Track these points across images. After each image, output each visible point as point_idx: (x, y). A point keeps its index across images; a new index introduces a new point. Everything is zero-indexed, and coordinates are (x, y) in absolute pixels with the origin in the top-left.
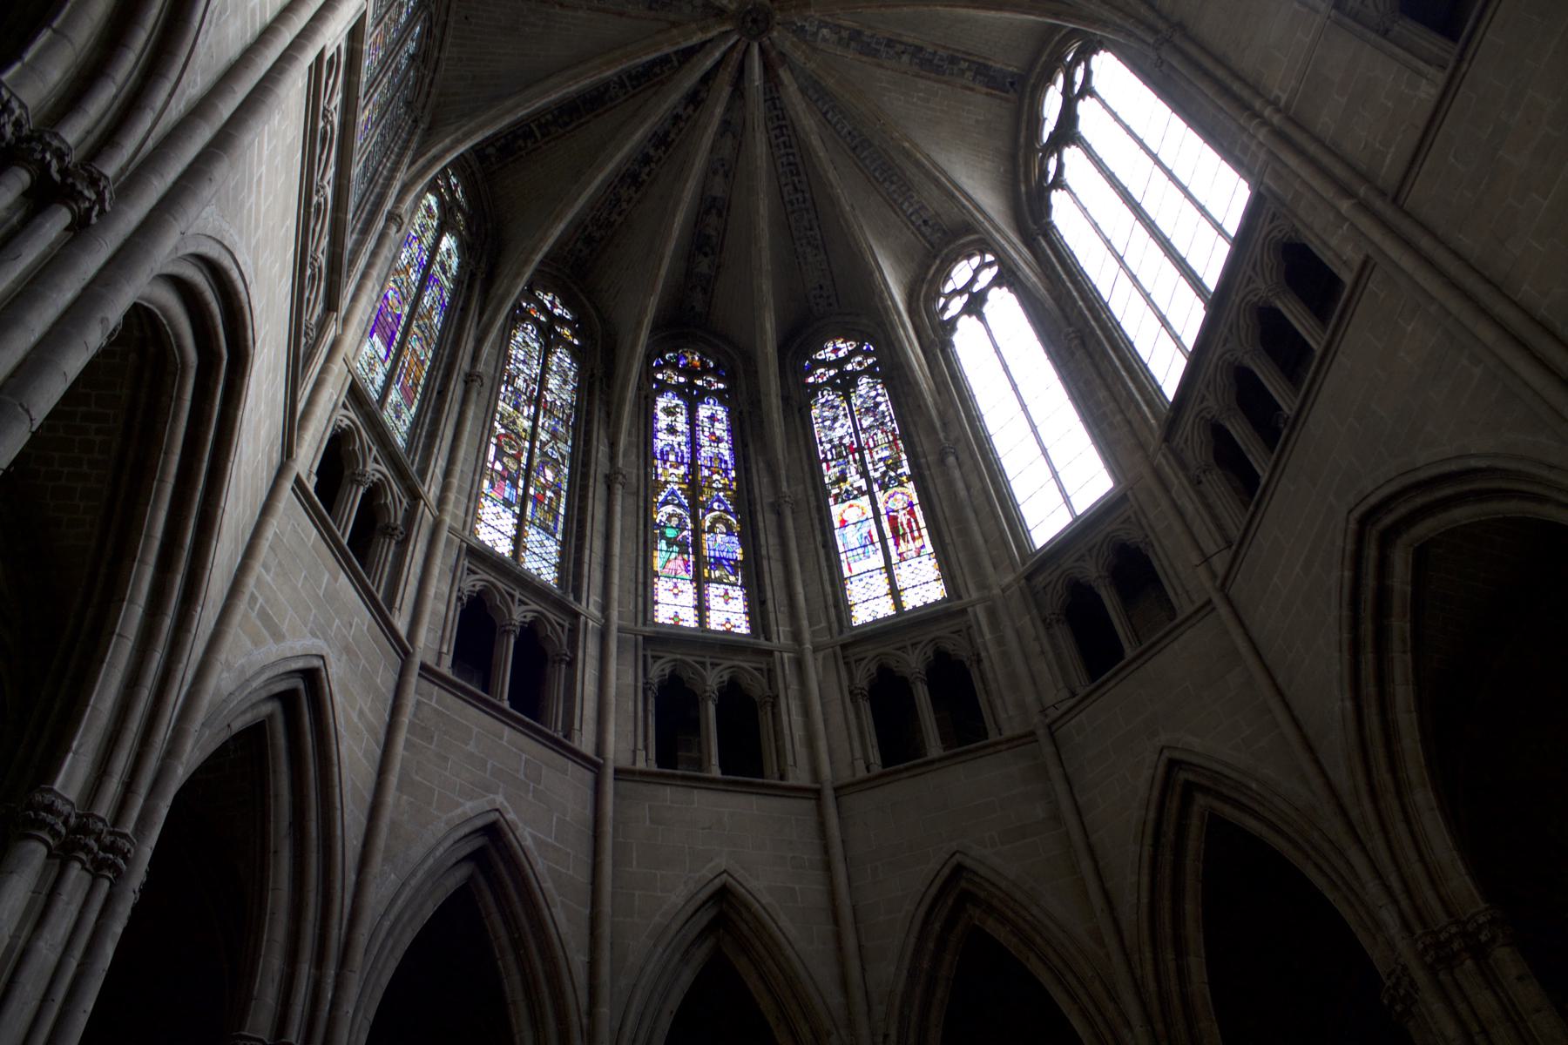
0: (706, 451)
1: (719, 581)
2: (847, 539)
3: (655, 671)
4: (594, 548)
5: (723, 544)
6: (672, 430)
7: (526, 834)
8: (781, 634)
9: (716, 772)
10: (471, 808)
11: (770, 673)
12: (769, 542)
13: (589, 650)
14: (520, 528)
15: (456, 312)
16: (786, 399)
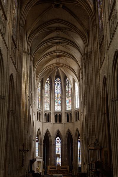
0: (59, 92)
1: (59, 106)
2: (67, 101)
3: (55, 115)
4: (51, 107)
5: (60, 102)
6: (56, 90)
7: (49, 129)
8: (62, 110)
9: (58, 123)
10: (46, 129)
11: (61, 114)
12: (62, 102)
13: (51, 114)
14: (47, 106)
15: (41, 88)
16: (64, 85)
